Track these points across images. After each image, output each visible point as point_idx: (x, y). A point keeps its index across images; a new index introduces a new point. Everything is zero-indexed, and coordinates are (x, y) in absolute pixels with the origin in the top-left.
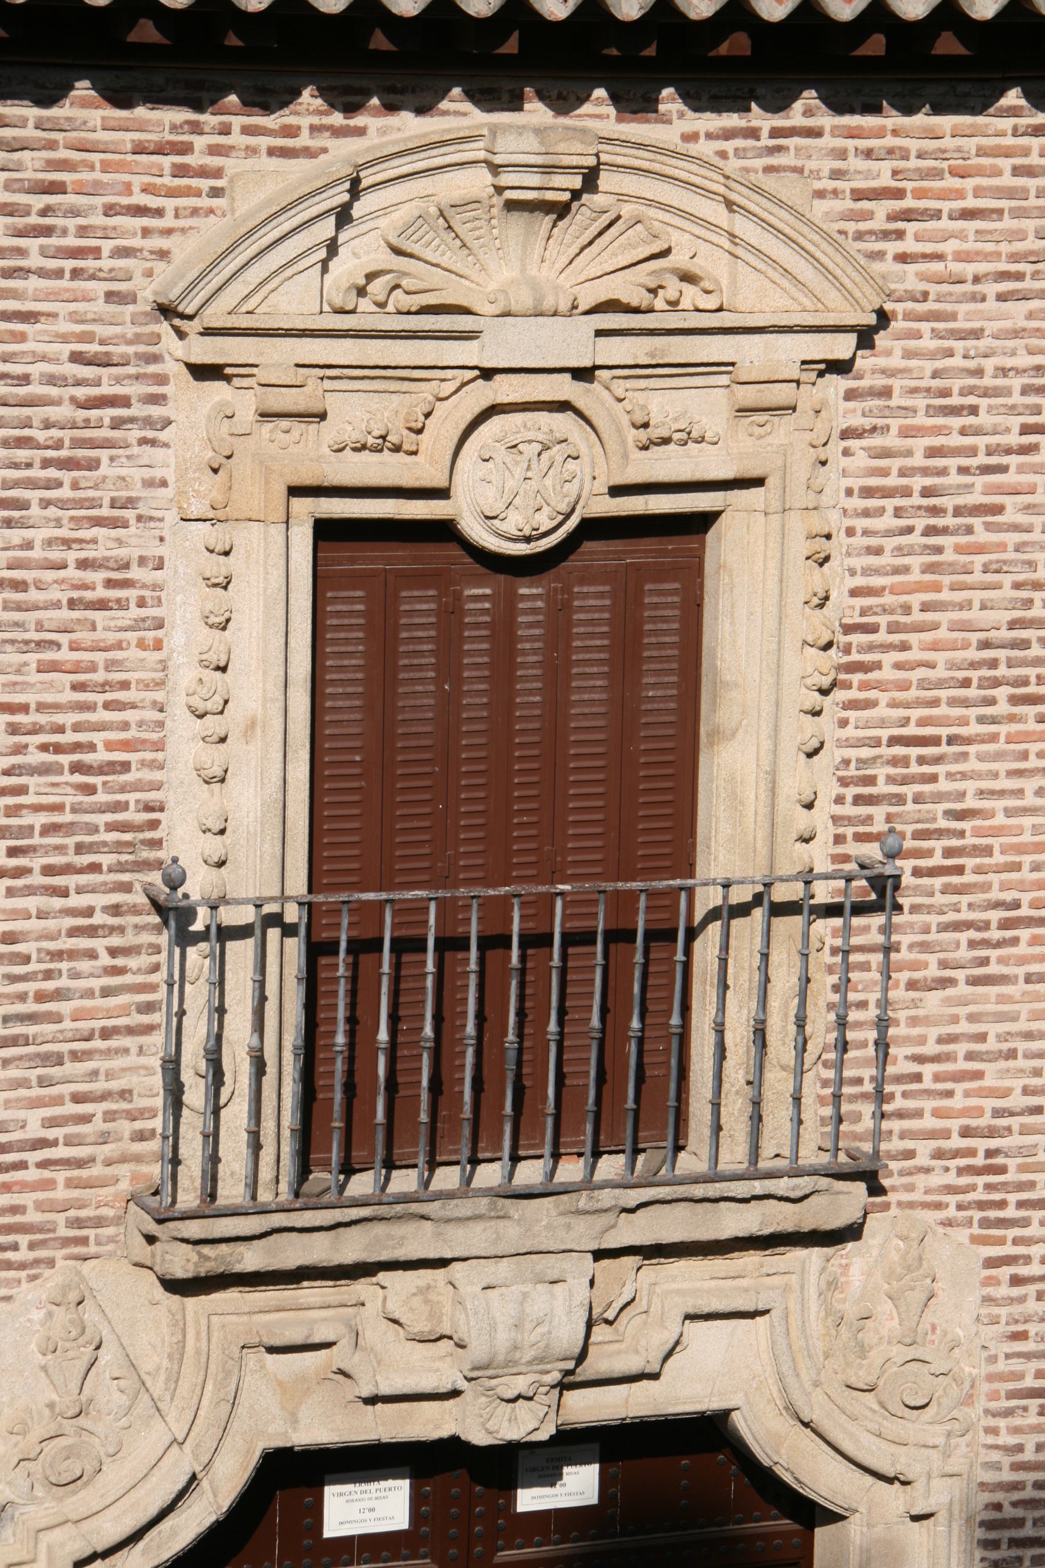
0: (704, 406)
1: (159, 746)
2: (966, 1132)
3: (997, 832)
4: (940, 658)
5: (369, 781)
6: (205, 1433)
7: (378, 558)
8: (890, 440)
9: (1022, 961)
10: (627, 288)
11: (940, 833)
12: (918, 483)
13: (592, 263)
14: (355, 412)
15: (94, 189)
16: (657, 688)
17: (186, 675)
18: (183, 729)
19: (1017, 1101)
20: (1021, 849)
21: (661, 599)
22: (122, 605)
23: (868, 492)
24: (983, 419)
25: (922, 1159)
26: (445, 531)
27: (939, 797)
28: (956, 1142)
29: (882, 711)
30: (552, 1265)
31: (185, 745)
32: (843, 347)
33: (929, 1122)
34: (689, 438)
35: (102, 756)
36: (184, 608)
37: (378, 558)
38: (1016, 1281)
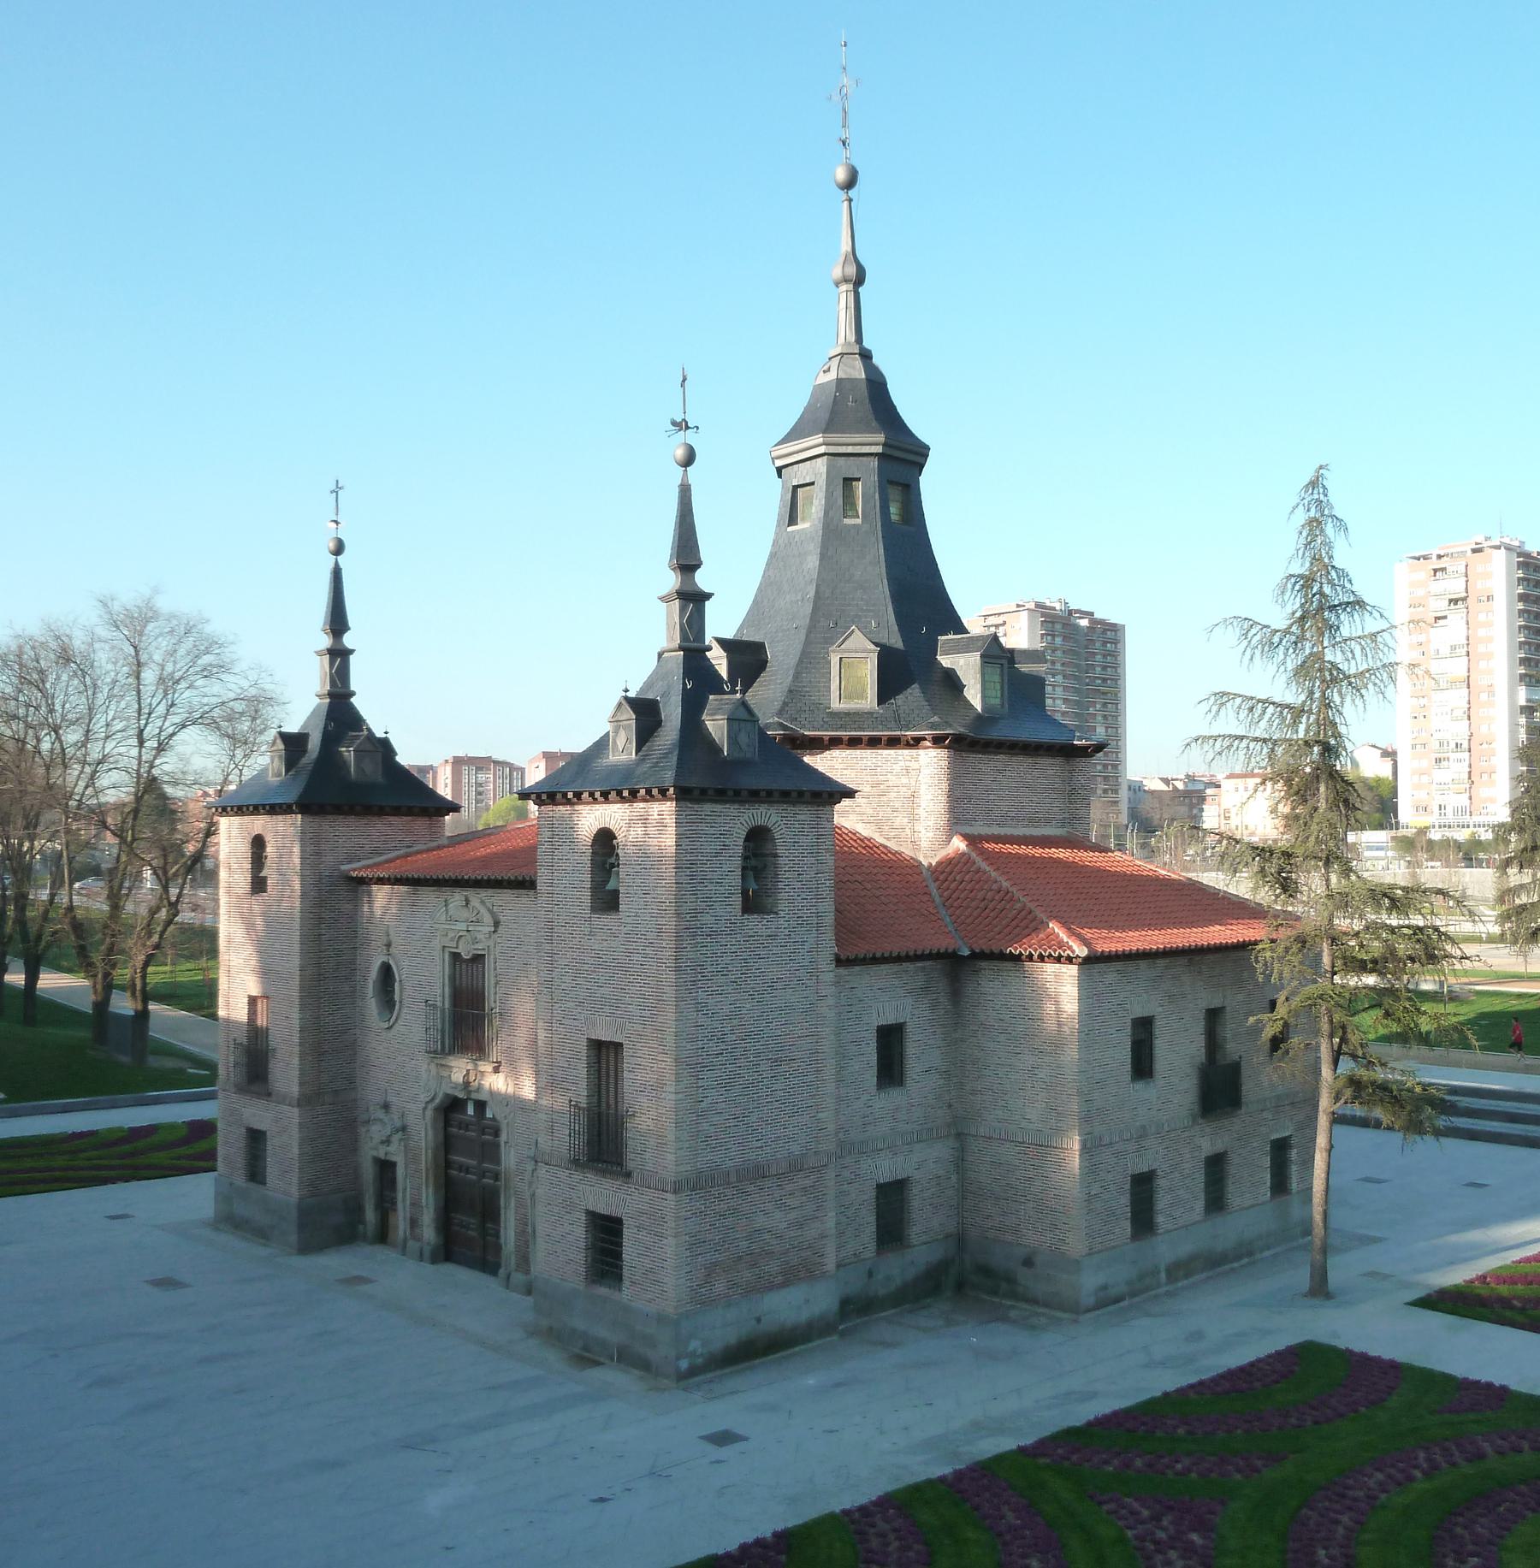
37: (456, 957)
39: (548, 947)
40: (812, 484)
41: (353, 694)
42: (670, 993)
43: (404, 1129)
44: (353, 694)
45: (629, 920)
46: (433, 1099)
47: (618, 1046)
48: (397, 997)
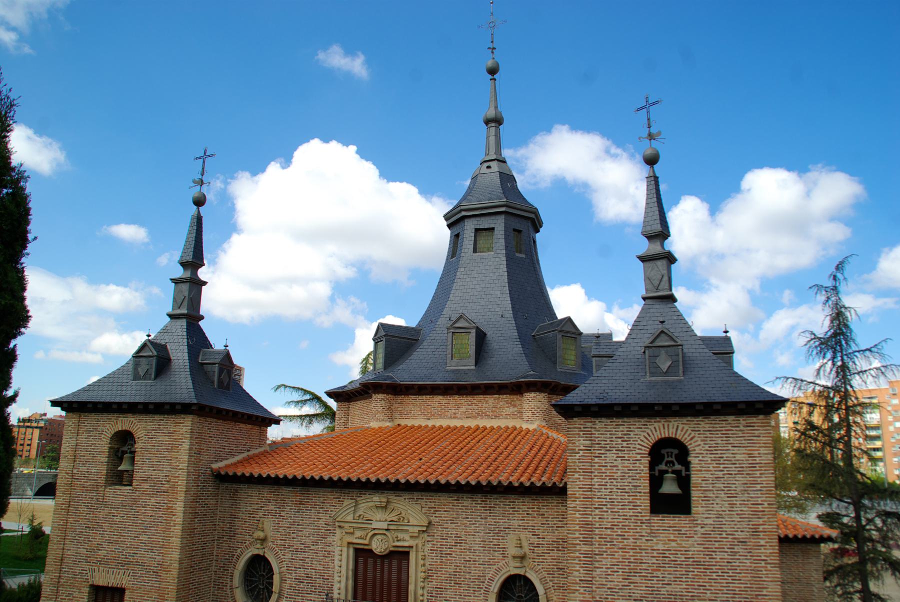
0: (407, 536)
7: (362, 554)
10: (395, 519)
14: (358, 533)
16: (404, 577)
17: (337, 568)
18: (336, 575)
26: (371, 551)
31: (337, 578)
32: (424, 529)
34: (404, 540)
36: (337, 558)
37: (362, 554)
39: (585, 548)
40: (493, 229)
41: (202, 318)
44: (202, 318)
45: (710, 521)
48: (275, 588)
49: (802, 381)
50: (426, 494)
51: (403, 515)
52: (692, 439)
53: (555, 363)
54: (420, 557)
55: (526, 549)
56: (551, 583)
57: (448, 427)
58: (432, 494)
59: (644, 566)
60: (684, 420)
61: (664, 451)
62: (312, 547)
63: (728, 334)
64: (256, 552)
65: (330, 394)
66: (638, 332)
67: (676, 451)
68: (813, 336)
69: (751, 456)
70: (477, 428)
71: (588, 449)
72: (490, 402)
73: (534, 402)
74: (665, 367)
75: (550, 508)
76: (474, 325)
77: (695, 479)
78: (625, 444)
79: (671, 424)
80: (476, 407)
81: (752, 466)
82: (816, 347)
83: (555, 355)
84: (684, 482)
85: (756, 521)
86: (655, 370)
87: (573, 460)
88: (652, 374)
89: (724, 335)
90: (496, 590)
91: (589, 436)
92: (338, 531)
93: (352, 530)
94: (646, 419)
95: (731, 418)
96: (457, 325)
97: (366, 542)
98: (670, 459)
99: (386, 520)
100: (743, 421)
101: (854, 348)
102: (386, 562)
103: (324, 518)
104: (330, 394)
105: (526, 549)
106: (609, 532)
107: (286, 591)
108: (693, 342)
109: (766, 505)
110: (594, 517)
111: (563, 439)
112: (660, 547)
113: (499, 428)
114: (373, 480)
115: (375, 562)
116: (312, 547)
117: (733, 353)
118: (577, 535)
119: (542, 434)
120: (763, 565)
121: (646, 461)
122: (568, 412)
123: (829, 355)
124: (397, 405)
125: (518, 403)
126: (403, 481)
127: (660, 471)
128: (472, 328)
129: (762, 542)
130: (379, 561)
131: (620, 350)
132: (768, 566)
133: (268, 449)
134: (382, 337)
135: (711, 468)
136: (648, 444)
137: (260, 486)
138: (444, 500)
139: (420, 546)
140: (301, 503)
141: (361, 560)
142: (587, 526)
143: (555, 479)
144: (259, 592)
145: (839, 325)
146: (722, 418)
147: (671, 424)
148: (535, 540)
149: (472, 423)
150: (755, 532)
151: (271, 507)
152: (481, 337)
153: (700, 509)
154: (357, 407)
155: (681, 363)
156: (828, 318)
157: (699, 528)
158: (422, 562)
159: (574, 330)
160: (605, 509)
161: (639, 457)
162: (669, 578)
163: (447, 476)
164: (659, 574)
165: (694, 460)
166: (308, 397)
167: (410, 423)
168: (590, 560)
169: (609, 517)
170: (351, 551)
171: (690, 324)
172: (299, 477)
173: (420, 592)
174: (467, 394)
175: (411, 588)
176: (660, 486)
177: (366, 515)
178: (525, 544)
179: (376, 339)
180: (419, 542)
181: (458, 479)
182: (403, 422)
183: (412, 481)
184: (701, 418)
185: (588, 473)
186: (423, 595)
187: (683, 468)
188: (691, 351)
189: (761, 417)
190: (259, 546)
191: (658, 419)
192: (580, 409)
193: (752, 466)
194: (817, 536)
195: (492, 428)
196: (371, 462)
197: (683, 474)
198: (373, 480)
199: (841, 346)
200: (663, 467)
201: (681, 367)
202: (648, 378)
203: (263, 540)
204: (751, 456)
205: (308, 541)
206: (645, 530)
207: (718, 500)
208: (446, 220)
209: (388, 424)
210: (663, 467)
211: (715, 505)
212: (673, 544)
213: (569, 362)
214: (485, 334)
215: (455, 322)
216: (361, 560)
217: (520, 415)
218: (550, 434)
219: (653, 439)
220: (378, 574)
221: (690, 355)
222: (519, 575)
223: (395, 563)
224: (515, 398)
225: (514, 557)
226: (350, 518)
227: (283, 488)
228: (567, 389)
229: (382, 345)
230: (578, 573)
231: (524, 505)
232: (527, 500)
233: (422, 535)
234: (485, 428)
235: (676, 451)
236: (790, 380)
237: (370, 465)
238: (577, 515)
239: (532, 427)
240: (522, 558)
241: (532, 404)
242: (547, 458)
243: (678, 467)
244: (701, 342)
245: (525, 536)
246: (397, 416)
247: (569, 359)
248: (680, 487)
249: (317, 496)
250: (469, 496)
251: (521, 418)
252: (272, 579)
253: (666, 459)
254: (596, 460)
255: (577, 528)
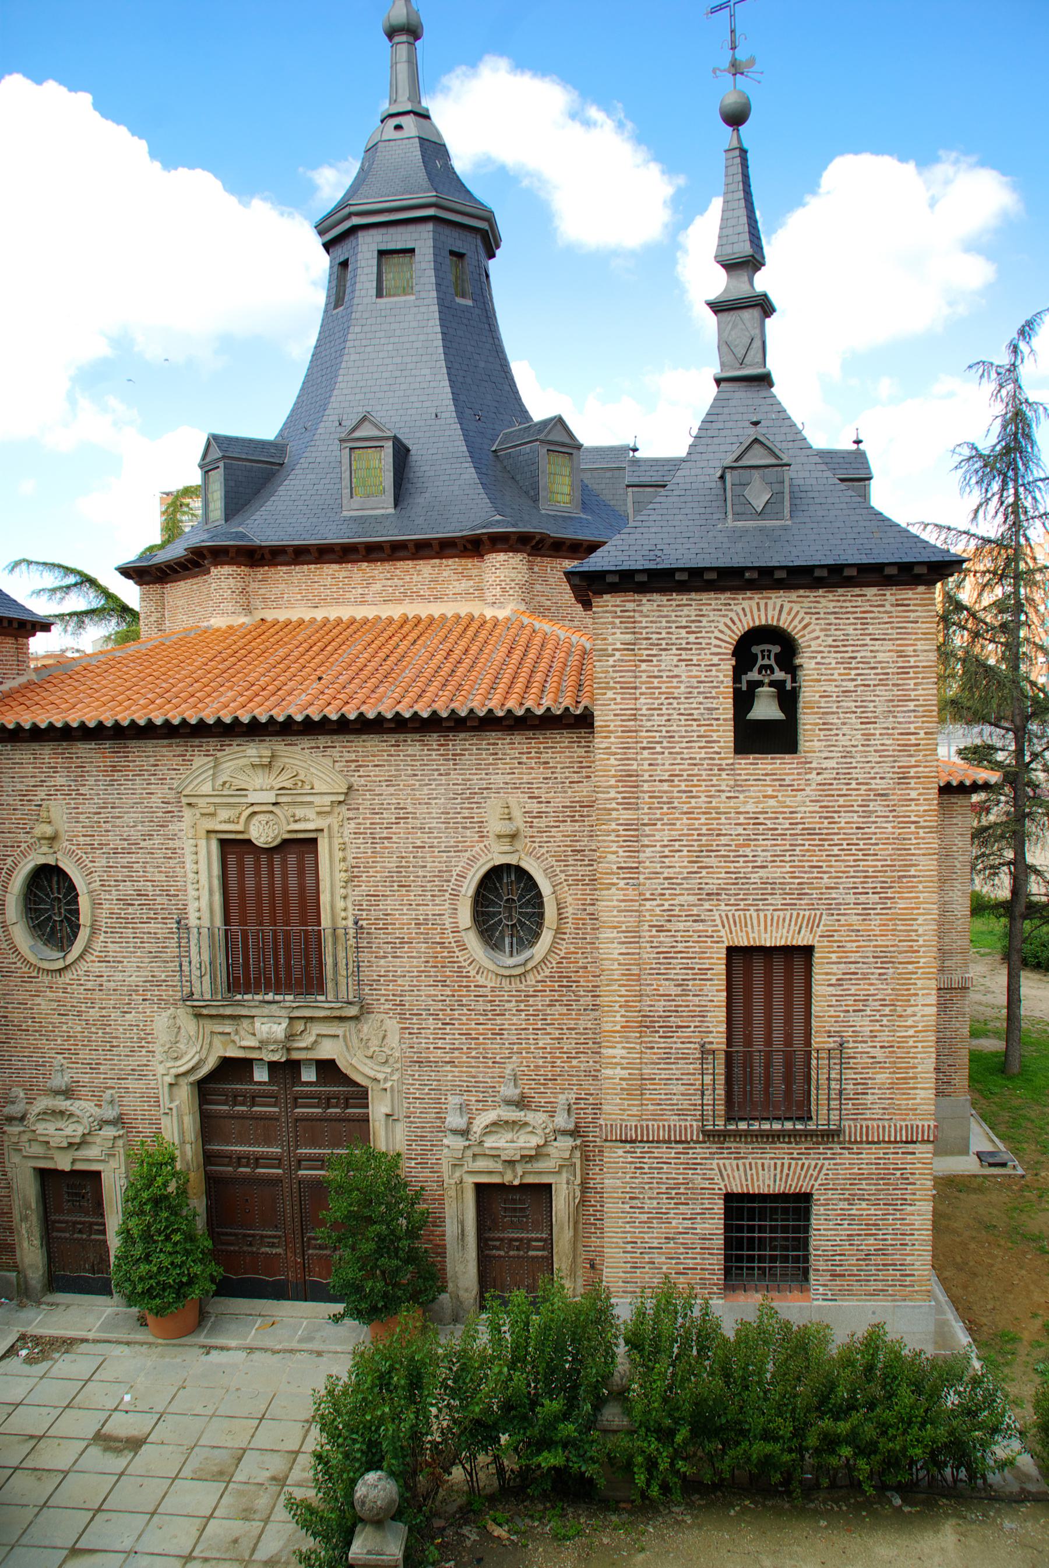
0: (310, 813)
1: (186, 891)
2: (393, 995)
3: (397, 919)
4: (378, 875)
5: (234, 903)
6: (204, 1052)
7: (233, 848)
8: (360, 821)
9: (406, 952)
10: (288, 784)
11: (382, 919)
12: (369, 831)
13: (281, 778)
14: (224, 814)
15: (166, 765)
16: (309, 881)
17: (191, 875)
18: (190, 887)
19: (407, 988)
20: (403, 924)
21: (308, 857)
22: (175, 858)
23: (355, 833)
24: (385, 816)
25: (382, 1001)
26: (249, 841)
27: (380, 910)
28: (391, 997)
29: (363, 888)
30: (279, 1020)
31: (192, 893)
32: (341, 798)
33: (383, 992)
35: (172, 892)
36: (189, 859)
37: (233, 848)
38: (410, 1033)
39: (626, 815)
40: (412, 251)
42: (926, 866)
43: (118, 1121)
45: (832, 764)
46: (194, 1069)
47: (807, 952)
48: (84, 919)
49: (949, 529)
50: (341, 738)
51: (301, 777)
52: (805, 627)
53: (535, 500)
54: (337, 847)
55: (519, 822)
56: (563, 876)
57: (353, 621)
58: (351, 737)
59: (724, 840)
60: (793, 595)
61: (756, 649)
62: (143, 844)
63: (860, 445)
64: (42, 860)
65: (127, 572)
66: (709, 441)
67: (776, 649)
68: (974, 453)
69: (901, 654)
70: (405, 620)
71: (629, 647)
72: (426, 569)
73: (503, 569)
74: (759, 504)
75: (560, 750)
76: (389, 434)
77: (808, 694)
78: (692, 638)
79: (770, 603)
80: (401, 583)
81: (903, 671)
82: (977, 472)
83: (535, 487)
84: (788, 699)
85: (904, 761)
86: (745, 509)
87: (602, 668)
88: (738, 516)
89: (855, 446)
90: (471, 892)
91: (631, 625)
92: (187, 813)
93: (212, 810)
94: (728, 595)
95: (871, 592)
96: (357, 434)
97: (240, 827)
98: (766, 662)
99: (272, 788)
100: (891, 595)
101: (1038, 473)
102: (277, 858)
103: (161, 792)
104: (127, 572)
105: (519, 822)
106: (665, 786)
107: (103, 923)
108: (805, 460)
109: (922, 735)
110: (640, 764)
111: (562, 634)
112: (750, 807)
113: (443, 617)
114: (245, 719)
115: (257, 861)
116: (143, 844)
117: (870, 479)
118: (612, 795)
119: (523, 627)
120: (913, 829)
121: (728, 666)
122: (589, 587)
123: (995, 486)
124: (256, 585)
125: (474, 572)
126: (299, 718)
127: (748, 682)
128: (387, 439)
129: (914, 794)
130: (264, 858)
131: (679, 473)
132: (921, 831)
133: (34, 677)
134: (218, 460)
135: (836, 677)
136: (732, 637)
137: (35, 746)
138: (371, 745)
139: (336, 827)
140: (114, 769)
141: (232, 859)
142: (629, 779)
143: (567, 702)
144: (53, 928)
145: (1016, 434)
146: (857, 591)
147: (770, 603)
148: (533, 806)
149: (396, 611)
150: (903, 778)
151: (60, 780)
152: (402, 454)
153: (816, 743)
154: (180, 592)
155: (787, 497)
156: (999, 421)
157: (813, 775)
158: (341, 854)
159: (567, 440)
160: (659, 749)
161: (715, 660)
162: (763, 856)
163: (375, 705)
164: (748, 851)
165: (807, 662)
166: (72, 579)
167: (282, 615)
168: (634, 835)
169: (665, 762)
170: (215, 846)
171: (800, 427)
172: (109, 723)
173: (340, 904)
174: (382, 560)
175: (325, 898)
176: (750, 708)
177: (235, 782)
178: (517, 813)
179: (207, 467)
180: (333, 820)
181: (398, 708)
182: (270, 615)
183: (316, 718)
184: (821, 592)
185: (630, 688)
186: (345, 910)
187: (789, 677)
188: (801, 475)
189: (921, 589)
190: (45, 849)
191: (749, 594)
192: (616, 579)
193: (903, 671)
194: (968, 783)
195: (431, 619)
196: (231, 688)
197: (788, 687)
198: (245, 719)
199: (1016, 469)
200: (754, 675)
201: (787, 504)
202: (730, 523)
203: (53, 839)
204: (901, 654)
205: (135, 834)
206: (725, 781)
207: (845, 729)
208: (321, 233)
209: (243, 619)
210: (754, 675)
211: (840, 737)
212: (772, 802)
213: (559, 498)
214: (408, 450)
215: (354, 430)
216: (232, 859)
217: (479, 593)
218: (537, 625)
219: (740, 629)
220: (265, 881)
221: (801, 482)
222: (509, 866)
223: (292, 859)
224: (469, 563)
225: (499, 836)
226: (206, 788)
227: (80, 745)
228: (593, 547)
229: (218, 476)
230: (614, 856)
231: (512, 748)
232: (518, 738)
233: (337, 810)
234: (419, 621)
235: (776, 649)
236: (930, 528)
237: (230, 694)
238: (612, 762)
239: (502, 614)
240: (513, 837)
241: (502, 574)
242: (543, 666)
243: (779, 675)
244: (817, 459)
245: (518, 802)
246: (258, 603)
247: (559, 490)
248: (782, 707)
249: (145, 755)
250: (417, 736)
251: (482, 598)
252: (77, 903)
253: (760, 662)
254: (644, 666)
255: (613, 782)
